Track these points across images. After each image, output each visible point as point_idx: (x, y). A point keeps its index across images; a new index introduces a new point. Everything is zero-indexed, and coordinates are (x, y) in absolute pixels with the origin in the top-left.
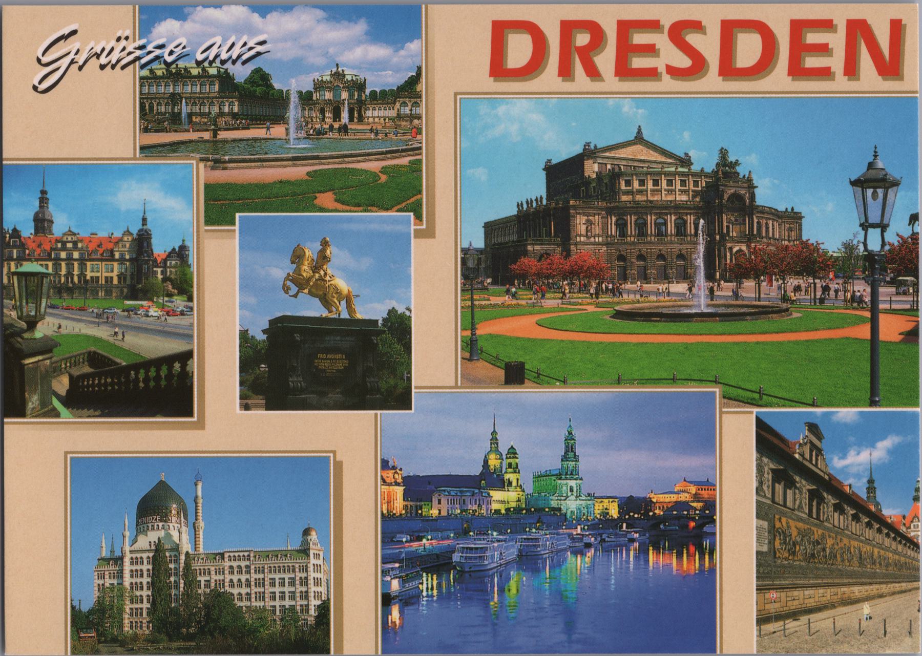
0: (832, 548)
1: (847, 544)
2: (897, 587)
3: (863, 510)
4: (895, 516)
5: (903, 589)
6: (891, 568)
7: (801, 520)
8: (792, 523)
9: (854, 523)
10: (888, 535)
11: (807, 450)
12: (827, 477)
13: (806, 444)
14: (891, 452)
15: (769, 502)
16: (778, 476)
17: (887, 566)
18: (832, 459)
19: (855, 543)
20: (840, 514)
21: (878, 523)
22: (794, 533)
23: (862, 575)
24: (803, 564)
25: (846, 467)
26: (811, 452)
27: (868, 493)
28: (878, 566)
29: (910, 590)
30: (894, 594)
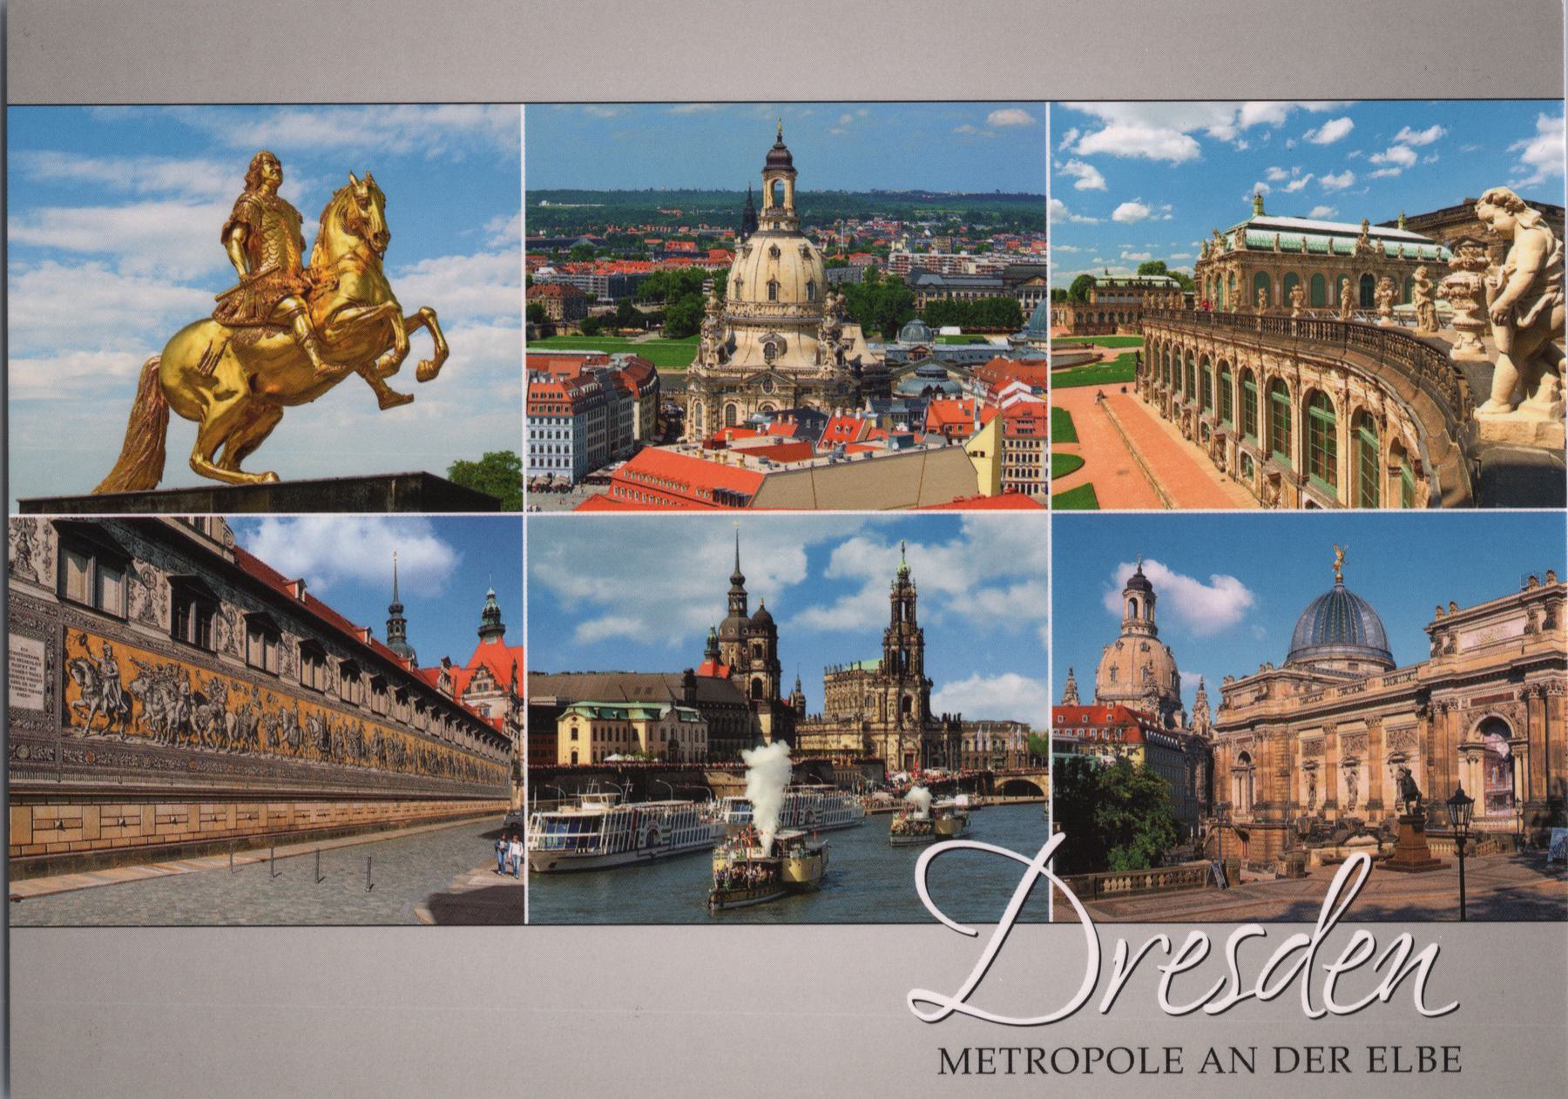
6: (409, 768)
7: (148, 645)
12: (230, 558)
17: (401, 762)
19: (314, 709)
22: (128, 673)
24: (153, 743)
28: (375, 760)
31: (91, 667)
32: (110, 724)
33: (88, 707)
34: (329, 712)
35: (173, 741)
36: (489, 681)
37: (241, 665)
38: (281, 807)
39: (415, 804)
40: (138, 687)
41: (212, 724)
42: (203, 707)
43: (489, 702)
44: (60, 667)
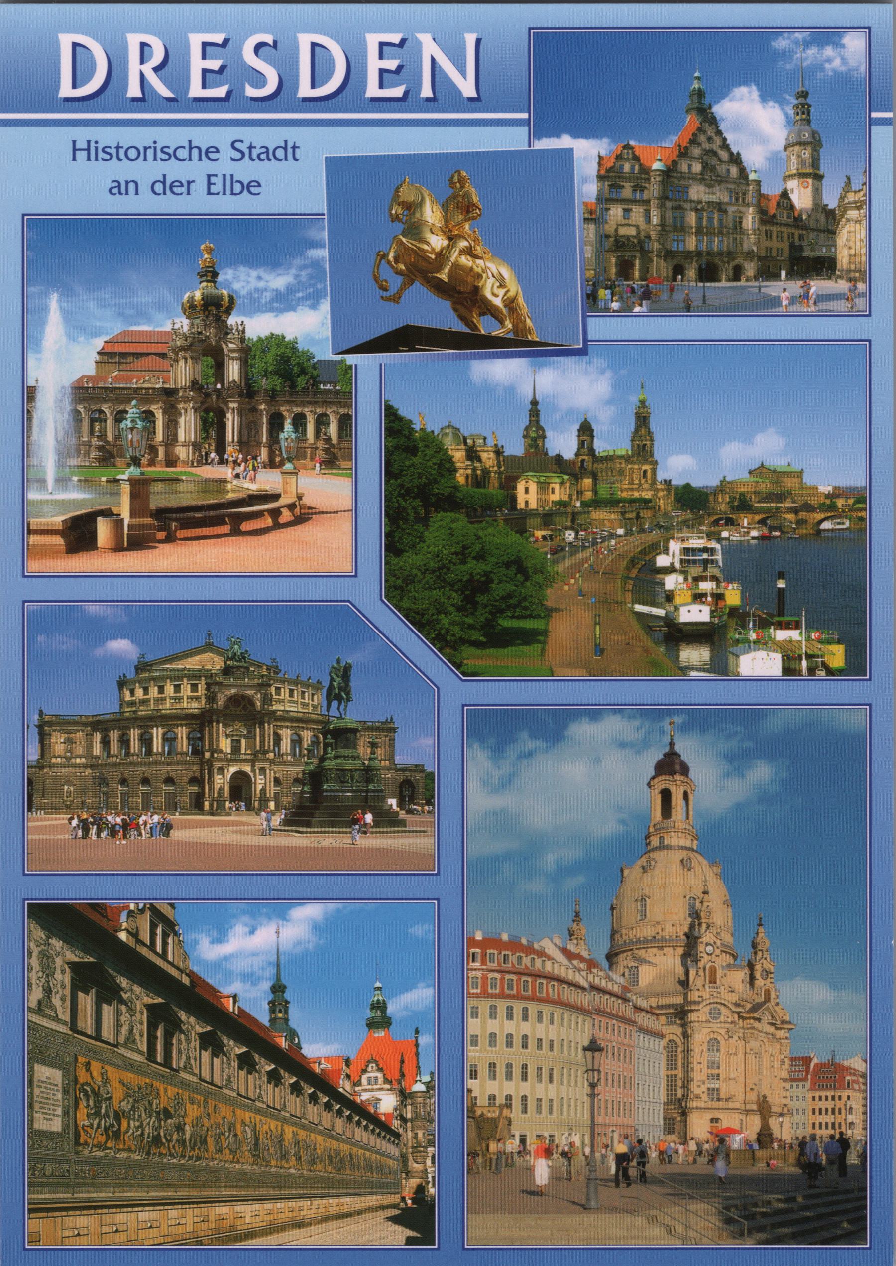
2: (333, 1205)
3: (263, 1046)
4: (327, 1059)
5: (345, 1209)
6: (319, 1167)
7: (129, 1066)
9: (243, 1073)
10: (313, 1098)
11: (144, 924)
12: (186, 980)
13: (142, 911)
14: (317, 928)
16: (83, 977)
17: (313, 1162)
18: (196, 942)
19: (247, 1116)
20: (215, 1055)
22: (118, 1093)
24: (136, 1157)
25: (226, 958)
26: (153, 927)
27: (272, 1011)
29: (360, 1213)
30: (326, 1219)
31: (93, 1091)
32: (107, 1140)
33: (91, 1126)
34: (258, 1117)
35: (148, 1154)
36: (379, 1075)
37: (195, 1079)
38: (223, 1210)
39: (324, 1201)
40: (126, 1106)
41: (175, 1137)
42: (169, 1121)
43: (378, 1094)
44: (73, 1089)
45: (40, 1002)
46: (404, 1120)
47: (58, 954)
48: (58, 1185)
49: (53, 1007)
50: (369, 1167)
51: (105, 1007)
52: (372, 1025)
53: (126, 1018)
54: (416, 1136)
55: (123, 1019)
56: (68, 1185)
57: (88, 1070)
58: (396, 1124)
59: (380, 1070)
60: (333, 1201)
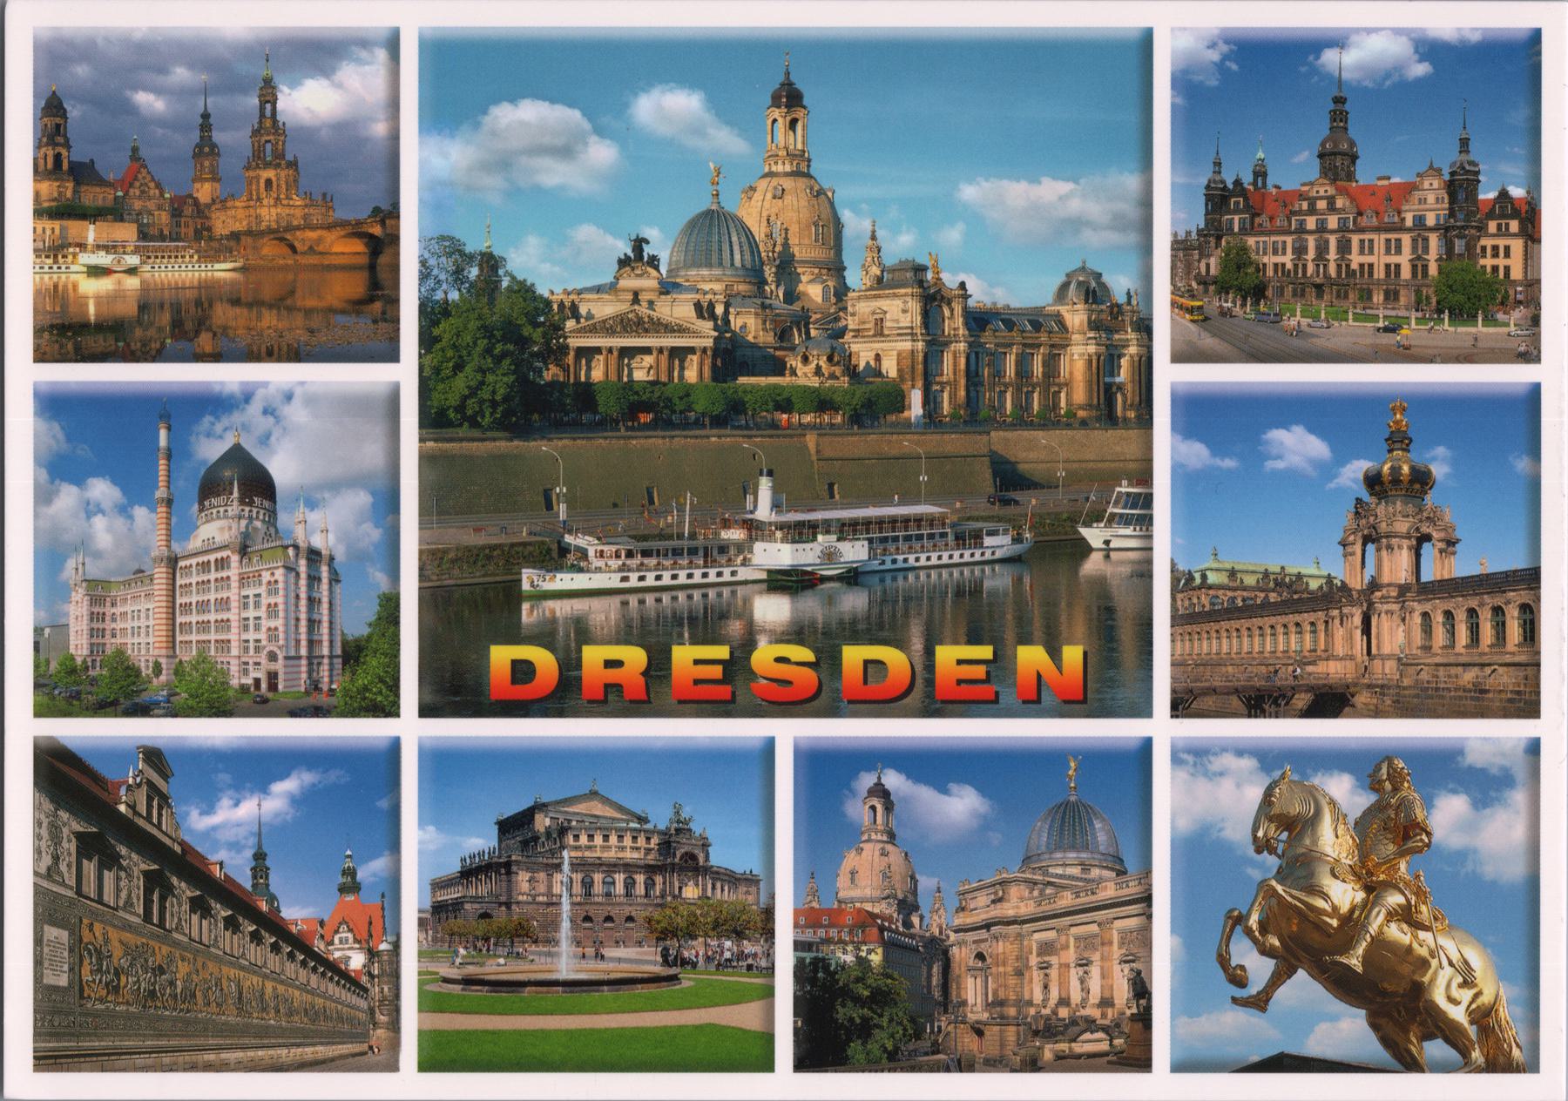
0: (187, 980)
1: (216, 971)
3: (246, 909)
4: (304, 921)
5: (320, 1056)
6: (296, 1018)
7: (127, 927)
8: (114, 935)
9: (228, 934)
10: (291, 956)
12: (178, 849)
13: (139, 785)
15: (70, 893)
16: (88, 846)
17: (290, 1013)
18: (187, 814)
19: (232, 972)
20: (203, 917)
21: (272, 933)
22: (117, 952)
23: (244, 1031)
24: (132, 1009)
25: (214, 828)
26: (150, 799)
27: (254, 877)
36: (350, 935)
37: (186, 939)
45: (49, 869)
46: (371, 976)
47: (65, 825)
48: (64, 1034)
49: (60, 874)
50: (340, 1019)
51: (106, 872)
52: (343, 890)
53: (124, 884)
54: (382, 991)
55: (122, 884)
56: (73, 1035)
57: (91, 930)
58: (364, 979)
59: (350, 930)
60: (309, 1050)
